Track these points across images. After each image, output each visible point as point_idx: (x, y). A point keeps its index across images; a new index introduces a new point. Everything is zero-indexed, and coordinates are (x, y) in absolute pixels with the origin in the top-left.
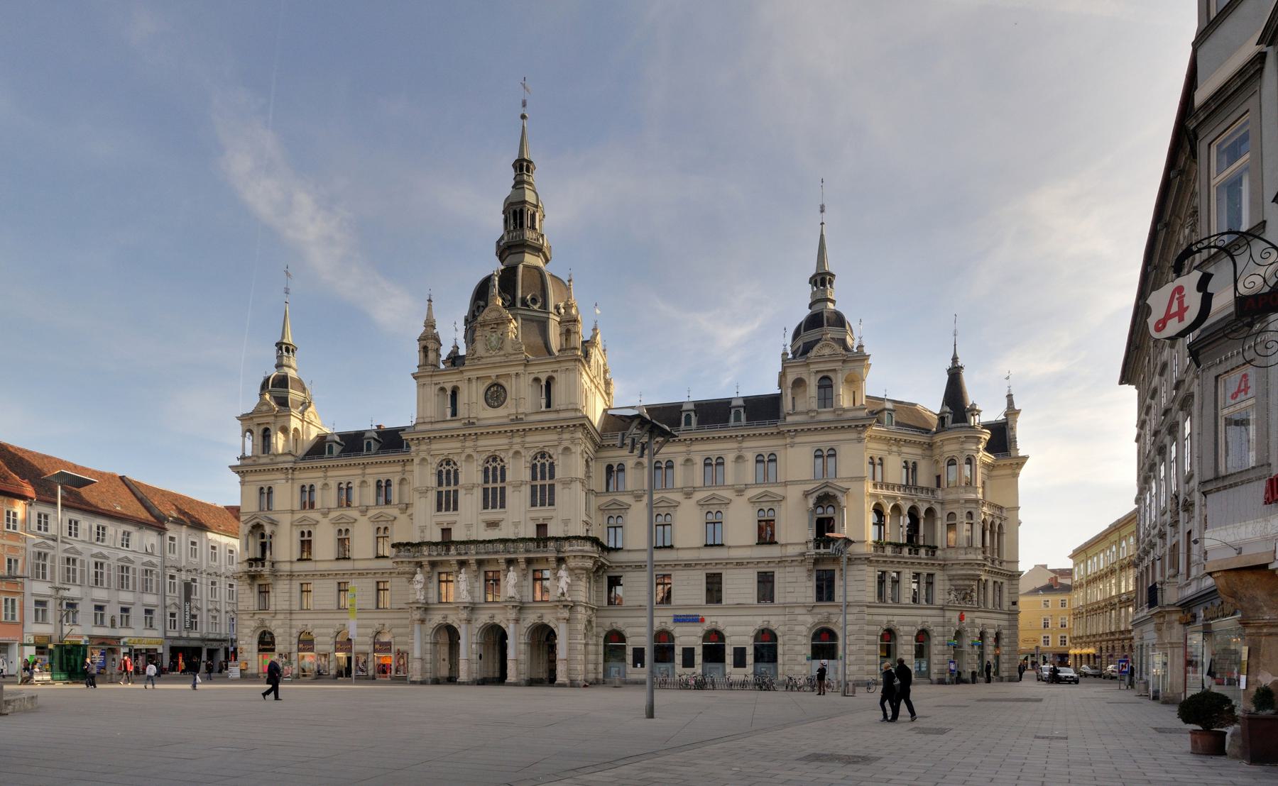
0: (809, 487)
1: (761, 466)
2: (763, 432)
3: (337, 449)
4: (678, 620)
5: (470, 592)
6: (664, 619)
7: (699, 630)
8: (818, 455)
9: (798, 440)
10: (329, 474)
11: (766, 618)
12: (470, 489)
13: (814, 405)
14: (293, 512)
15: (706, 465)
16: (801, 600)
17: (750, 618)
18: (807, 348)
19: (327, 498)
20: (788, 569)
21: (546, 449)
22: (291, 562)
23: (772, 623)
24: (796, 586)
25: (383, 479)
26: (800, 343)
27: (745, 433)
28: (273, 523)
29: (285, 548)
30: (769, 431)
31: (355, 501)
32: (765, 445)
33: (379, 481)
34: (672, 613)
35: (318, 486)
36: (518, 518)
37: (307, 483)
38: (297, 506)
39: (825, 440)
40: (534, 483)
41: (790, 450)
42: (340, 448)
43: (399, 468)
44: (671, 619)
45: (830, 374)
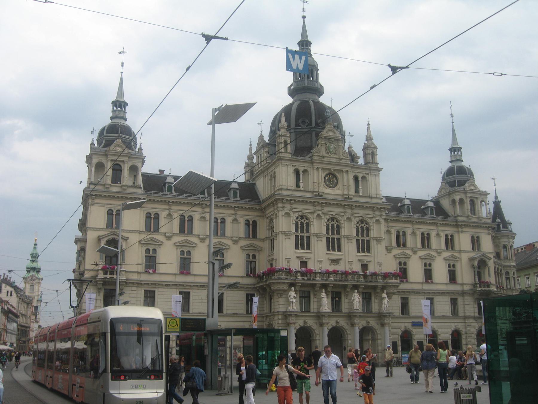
4: (415, 324)
6: (406, 324)
9: (464, 229)
11: (456, 324)
13: (470, 214)
14: (140, 232)
16: (472, 315)
17: (449, 324)
18: (462, 183)
19: (169, 225)
20: (466, 297)
22: (138, 273)
23: (459, 327)
28: (126, 239)
29: (133, 260)
32: (449, 230)
34: (411, 321)
36: (350, 259)
37: (153, 212)
38: (143, 228)
41: (461, 234)
44: (410, 325)
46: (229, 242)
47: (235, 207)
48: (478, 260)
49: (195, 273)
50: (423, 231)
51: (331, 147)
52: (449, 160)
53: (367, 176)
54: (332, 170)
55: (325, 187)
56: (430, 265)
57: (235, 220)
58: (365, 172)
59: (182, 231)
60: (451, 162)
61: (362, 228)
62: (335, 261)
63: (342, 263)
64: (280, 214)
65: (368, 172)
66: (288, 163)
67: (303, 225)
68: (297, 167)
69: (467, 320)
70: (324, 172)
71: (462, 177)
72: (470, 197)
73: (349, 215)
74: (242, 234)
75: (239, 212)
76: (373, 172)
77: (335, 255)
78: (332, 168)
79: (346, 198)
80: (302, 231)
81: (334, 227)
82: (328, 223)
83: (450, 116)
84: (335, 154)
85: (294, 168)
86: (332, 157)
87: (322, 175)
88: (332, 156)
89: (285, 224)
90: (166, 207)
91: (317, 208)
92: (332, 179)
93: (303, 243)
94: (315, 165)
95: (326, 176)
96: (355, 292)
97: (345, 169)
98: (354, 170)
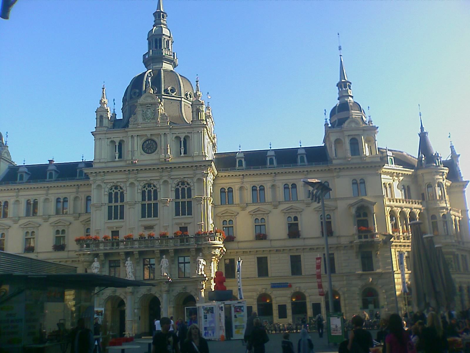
0: (352, 201)
1: (287, 190)
2: (320, 169)
3: (26, 177)
4: (274, 286)
5: (134, 273)
7: (288, 292)
8: (355, 183)
9: (341, 174)
10: (21, 193)
12: (99, 207)
15: (285, 188)
21: (186, 180)
24: (348, 262)
25: (62, 196)
26: (335, 118)
27: (309, 170)
30: (323, 168)
31: (40, 210)
33: (58, 199)
35: (11, 201)
39: (358, 174)
40: (178, 200)
42: (28, 177)
43: (74, 190)
44: (269, 287)
45: (356, 137)
46: (70, 218)
47: (74, 185)
48: (356, 206)
49: (38, 251)
50: (285, 182)
51: (148, 113)
52: (338, 96)
53: (189, 135)
54: (149, 136)
55: (141, 154)
56: (296, 218)
57: (76, 198)
58: (186, 131)
59: (28, 215)
60: (338, 99)
61: (183, 189)
62: (150, 228)
63: (156, 228)
64: (93, 186)
65: (190, 130)
66: (102, 136)
67: (116, 195)
68: (112, 139)
69: (345, 278)
70: (141, 139)
71: (343, 115)
72: (349, 136)
73: (165, 178)
74: (83, 211)
75: (80, 190)
76: (196, 130)
77: (149, 221)
78: (148, 133)
79: (162, 162)
80: (116, 201)
81: (150, 193)
82: (145, 189)
83: (338, 48)
84: (153, 119)
85: (110, 140)
86: (149, 123)
87: (138, 143)
88: (149, 121)
89: (100, 197)
90: (15, 194)
91: (130, 176)
92: (150, 146)
93: (116, 213)
94: (130, 134)
95: (145, 142)
96: (163, 258)
97: (162, 132)
98: (173, 131)
